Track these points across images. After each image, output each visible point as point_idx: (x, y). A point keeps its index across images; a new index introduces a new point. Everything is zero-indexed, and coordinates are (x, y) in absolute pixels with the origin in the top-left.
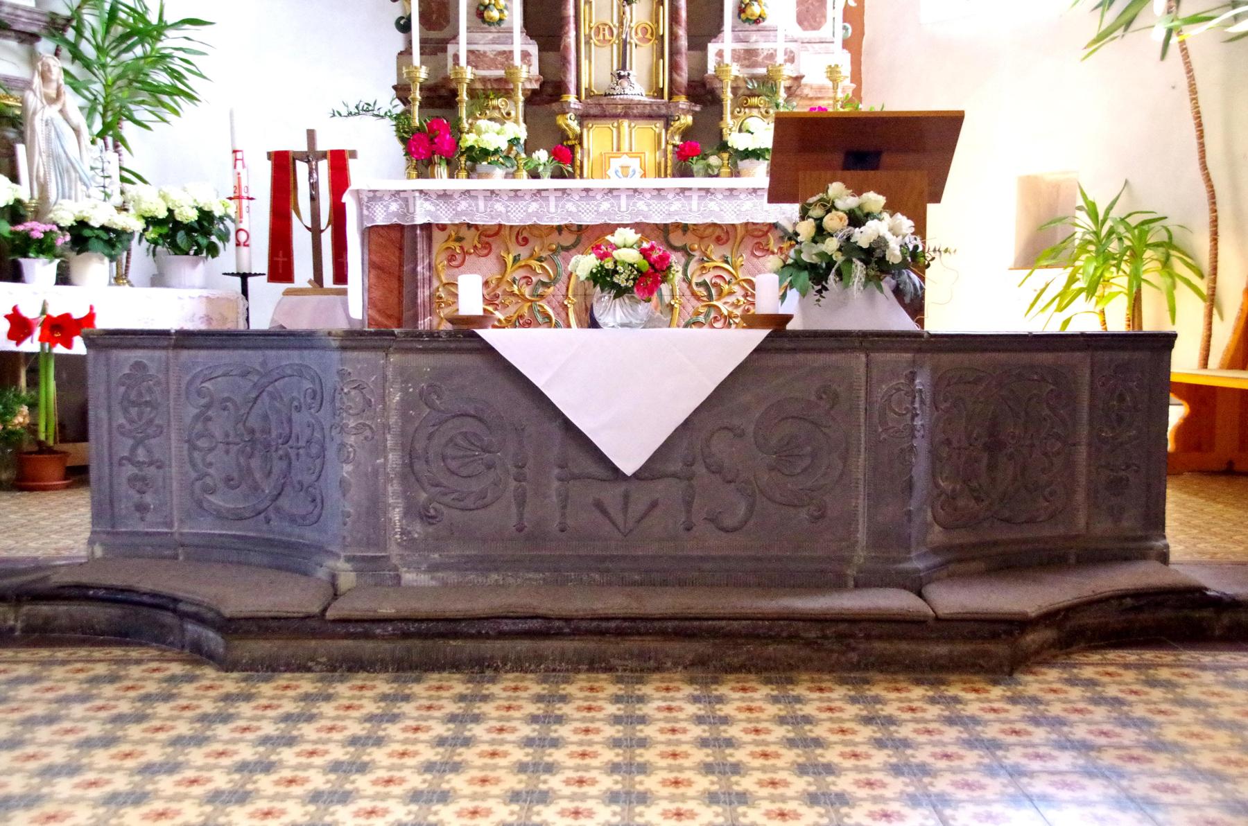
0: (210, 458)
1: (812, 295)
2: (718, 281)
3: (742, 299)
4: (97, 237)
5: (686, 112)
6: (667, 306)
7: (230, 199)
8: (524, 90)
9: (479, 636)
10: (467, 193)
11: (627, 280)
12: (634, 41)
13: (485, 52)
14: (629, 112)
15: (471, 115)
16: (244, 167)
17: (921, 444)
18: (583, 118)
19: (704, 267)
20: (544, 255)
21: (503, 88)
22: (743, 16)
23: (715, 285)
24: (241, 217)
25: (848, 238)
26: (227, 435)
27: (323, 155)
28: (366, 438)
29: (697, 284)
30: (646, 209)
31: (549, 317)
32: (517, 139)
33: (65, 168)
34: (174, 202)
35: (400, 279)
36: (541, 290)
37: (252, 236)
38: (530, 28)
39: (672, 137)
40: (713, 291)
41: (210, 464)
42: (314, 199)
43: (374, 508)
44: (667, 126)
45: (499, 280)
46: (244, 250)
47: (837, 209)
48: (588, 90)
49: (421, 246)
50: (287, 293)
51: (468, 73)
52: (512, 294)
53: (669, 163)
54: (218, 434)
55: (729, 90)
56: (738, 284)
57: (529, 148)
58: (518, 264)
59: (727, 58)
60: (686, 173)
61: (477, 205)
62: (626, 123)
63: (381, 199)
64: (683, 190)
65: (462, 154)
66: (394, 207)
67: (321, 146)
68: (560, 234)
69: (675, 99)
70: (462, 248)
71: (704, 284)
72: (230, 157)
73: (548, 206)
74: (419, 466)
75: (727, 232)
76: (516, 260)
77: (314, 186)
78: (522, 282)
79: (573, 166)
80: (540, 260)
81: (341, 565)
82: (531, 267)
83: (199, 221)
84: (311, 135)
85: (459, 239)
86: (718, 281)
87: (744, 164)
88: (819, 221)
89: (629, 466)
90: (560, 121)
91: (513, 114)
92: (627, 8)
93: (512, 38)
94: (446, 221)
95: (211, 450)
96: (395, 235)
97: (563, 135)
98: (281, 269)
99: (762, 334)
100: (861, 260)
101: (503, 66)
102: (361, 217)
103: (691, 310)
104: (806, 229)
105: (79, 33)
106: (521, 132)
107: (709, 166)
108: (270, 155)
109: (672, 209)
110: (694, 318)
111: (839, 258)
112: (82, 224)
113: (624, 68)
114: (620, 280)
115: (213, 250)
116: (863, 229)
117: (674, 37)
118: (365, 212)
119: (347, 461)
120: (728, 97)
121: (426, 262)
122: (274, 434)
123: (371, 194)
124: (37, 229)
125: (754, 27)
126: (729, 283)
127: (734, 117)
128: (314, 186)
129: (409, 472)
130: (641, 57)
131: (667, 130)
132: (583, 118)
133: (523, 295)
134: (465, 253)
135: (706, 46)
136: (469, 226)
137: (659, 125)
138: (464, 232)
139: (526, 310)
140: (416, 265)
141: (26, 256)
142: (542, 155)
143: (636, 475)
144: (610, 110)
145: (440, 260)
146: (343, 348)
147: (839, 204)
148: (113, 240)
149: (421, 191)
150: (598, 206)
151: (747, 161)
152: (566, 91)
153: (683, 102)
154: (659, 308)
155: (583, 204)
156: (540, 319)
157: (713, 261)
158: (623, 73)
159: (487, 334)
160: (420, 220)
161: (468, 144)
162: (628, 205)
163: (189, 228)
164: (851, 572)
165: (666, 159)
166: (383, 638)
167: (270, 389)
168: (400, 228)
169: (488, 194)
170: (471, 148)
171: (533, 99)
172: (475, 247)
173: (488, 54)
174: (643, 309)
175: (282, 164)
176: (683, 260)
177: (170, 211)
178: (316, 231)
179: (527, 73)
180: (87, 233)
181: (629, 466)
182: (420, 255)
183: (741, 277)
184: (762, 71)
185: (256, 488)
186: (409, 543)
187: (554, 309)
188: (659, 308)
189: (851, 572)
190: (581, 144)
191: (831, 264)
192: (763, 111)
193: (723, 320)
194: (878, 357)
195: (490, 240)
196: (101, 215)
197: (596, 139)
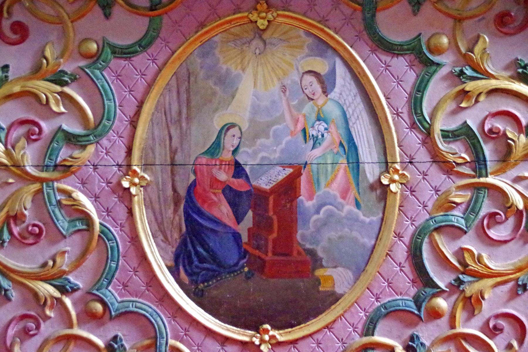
2: (499, 125)
6: (372, 188)
19: (464, 94)
29: (446, 135)
31: (87, 219)
40: (488, 150)
68: (107, 16)
78: (15, 134)
82: (36, 97)
86: (499, 125)
110: (439, 216)
133: (17, 166)
154: (353, 193)
156: (63, 224)
157: (490, 76)
176: (411, 77)
187: (95, 198)
188: (353, 193)
193: (511, 221)
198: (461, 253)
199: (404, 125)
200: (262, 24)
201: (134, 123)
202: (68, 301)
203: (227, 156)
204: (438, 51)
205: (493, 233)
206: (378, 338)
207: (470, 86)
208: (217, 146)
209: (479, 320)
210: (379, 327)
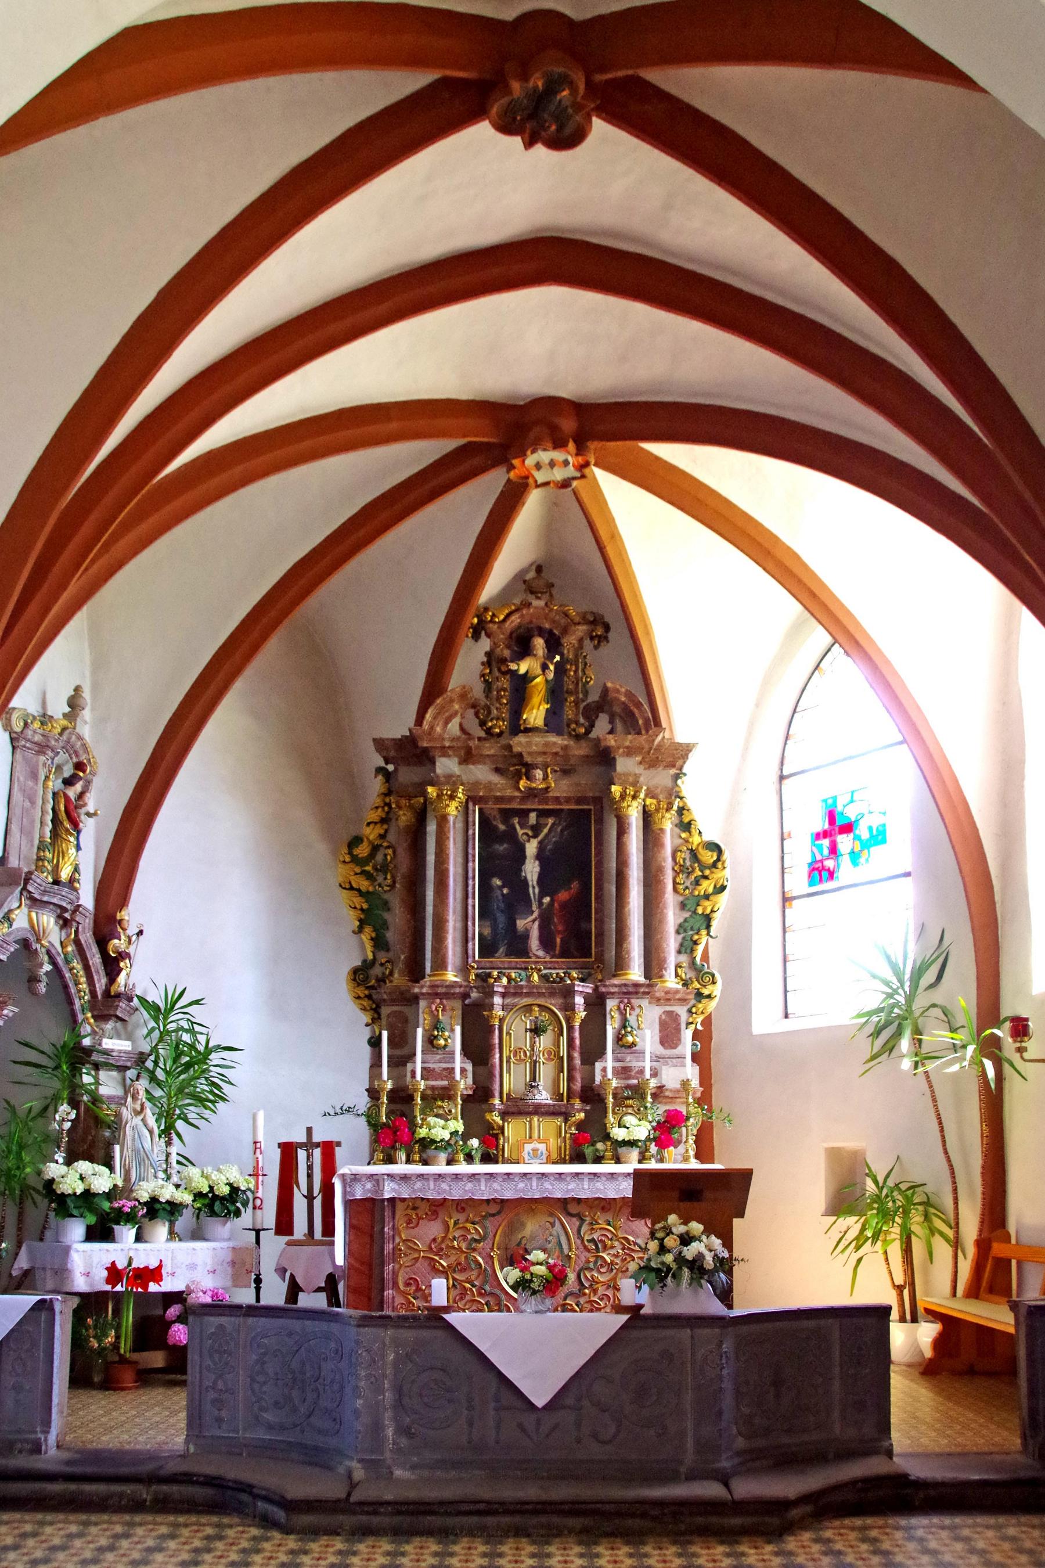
0: (264, 1389)
1: (658, 1287)
3: (621, 1251)
4: (164, 1209)
5: (579, 1111)
7: (250, 1175)
8: (462, 1095)
9: (447, 1514)
10: (421, 1176)
11: (539, 1286)
12: (542, 1060)
13: (434, 1069)
14: (539, 1110)
15: (423, 1112)
16: (261, 1153)
17: (727, 1385)
18: (504, 1115)
19: (593, 1229)
20: (477, 1220)
21: (446, 1094)
22: (620, 1043)
23: (601, 1241)
24: (258, 1188)
25: (680, 1253)
26: (277, 1374)
27: (318, 1145)
28: (372, 1383)
29: (588, 1241)
30: (550, 1187)
31: (480, 1264)
32: (457, 1132)
33: (142, 1157)
34: (213, 1181)
35: (372, 1236)
36: (474, 1245)
37: (264, 1202)
38: (467, 1051)
39: (570, 1128)
41: (265, 1392)
42: (310, 1176)
43: (377, 1427)
44: (566, 1121)
45: (444, 1238)
46: (258, 1212)
47: (673, 1234)
48: (508, 1095)
49: (387, 1213)
50: (289, 1244)
51: (422, 1085)
52: (453, 1247)
53: (568, 1147)
54: (270, 1371)
55: (611, 1096)
56: (618, 1240)
57: (466, 1136)
58: (457, 1226)
59: (610, 1075)
60: (578, 1158)
61: (428, 1185)
62: (536, 1119)
63: (359, 1180)
64: (577, 1174)
65: (416, 1142)
66: (369, 1186)
67: (316, 1138)
69: (572, 1102)
70: (417, 1215)
71: (593, 1241)
72: (252, 1146)
73: (479, 1185)
74: (406, 1401)
75: (609, 1203)
76: (456, 1223)
77: (310, 1168)
79: (497, 1150)
80: (473, 1223)
81: (354, 1464)
82: (466, 1228)
83: (230, 1194)
84: (309, 1130)
85: (415, 1208)
87: (622, 1150)
88: (662, 1240)
89: (540, 1402)
90: (488, 1117)
91: (453, 1111)
92: (537, 1039)
93: (454, 1058)
94: (406, 1196)
95: (265, 1383)
96: (368, 1205)
97: (490, 1126)
98: (284, 1225)
99: (624, 1318)
100: (688, 1268)
101: (447, 1078)
102: (345, 1193)
103: (583, 1259)
104: (653, 1246)
105: (156, 1063)
106: (459, 1126)
107: (597, 1150)
108: (280, 1145)
109: (569, 1187)
110: (586, 1265)
111: (674, 1266)
112: (154, 1199)
113: (533, 1079)
114: (535, 1286)
115: (238, 1213)
116: (689, 1247)
117: (570, 1058)
118: (348, 1189)
119: (359, 1397)
120: (610, 1100)
121: (391, 1225)
122: (308, 1375)
123: (353, 1177)
124: (127, 1205)
125: (628, 1051)
126: (611, 1240)
127: (614, 1113)
128: (310, 1168)
129: (399, 1405)
130: (546, 1072)
131: (566, 1123)
132: (504, 1115)
133: (460, 1248)
134: (420, 1218)
135: (594, 1065)
136: (423, 1199)
137: (559, 1121)
138: (418, 1203)
139: (463, 1260)
140: (383, 1228)
141: (118, 1224)
142: (475, 1143)
143: (545, 1407)
144: (523, 1109)
145: (401, 1224)
146: (359, 1326)
147: (674, 1230)
148: (173, 1208)
149: (388, 1175)
150: (516, 1186)
151: (624, 1148)
152: (493, 1096)
153: (577, 1104)
155: (505, 1184)
156: (473, 1266)
158: (533, 1084)
159: (451, 1318)
160: (387, 1196)
161: (422, 1136)
162: (537, 1186)
163: (222, 1199)
164: (683, 1469)
165: (565, 1146)
166: (385, 1514)
167: (306, 1345)
168: (371, 1200)
169: (437, 1177)
170: (424, 1139)
171: (466, 1099)
172: (426, 1214)
173: (436, 1070)
174: (549, 1302)
175: (288, 1151)
176: (578, 1223)
177: (211, 1188)
178: (310, 1198)
179: (464, 1084)
180: (157, 1206)
181: (540, 1402)
182: (387, 1220)
183: (620, 1236)
184: (635, 1082)
185: (295, 1410)
186: (398, 1450)
187: (483, 1259)
189: (683, 1469)
190: (503, 1133)
191: (669, 1269)
192: (636, 1109)
194: (699, 1331)
195: (438, 1209)
196: (167, 1193)
197: (513, 1130)
198: (592, 1276)
199: (576, 1237)
200: (534, 1207)
201: (495, 1236)
202: (474, 1289)
203: (523, 1246)
204: (586, 1216)
205: (602, 1270)
206: (568, 1302)
207: (594, 1227)
208: (520, 1243)
209: (597, 1296)
210: (569, 1298)
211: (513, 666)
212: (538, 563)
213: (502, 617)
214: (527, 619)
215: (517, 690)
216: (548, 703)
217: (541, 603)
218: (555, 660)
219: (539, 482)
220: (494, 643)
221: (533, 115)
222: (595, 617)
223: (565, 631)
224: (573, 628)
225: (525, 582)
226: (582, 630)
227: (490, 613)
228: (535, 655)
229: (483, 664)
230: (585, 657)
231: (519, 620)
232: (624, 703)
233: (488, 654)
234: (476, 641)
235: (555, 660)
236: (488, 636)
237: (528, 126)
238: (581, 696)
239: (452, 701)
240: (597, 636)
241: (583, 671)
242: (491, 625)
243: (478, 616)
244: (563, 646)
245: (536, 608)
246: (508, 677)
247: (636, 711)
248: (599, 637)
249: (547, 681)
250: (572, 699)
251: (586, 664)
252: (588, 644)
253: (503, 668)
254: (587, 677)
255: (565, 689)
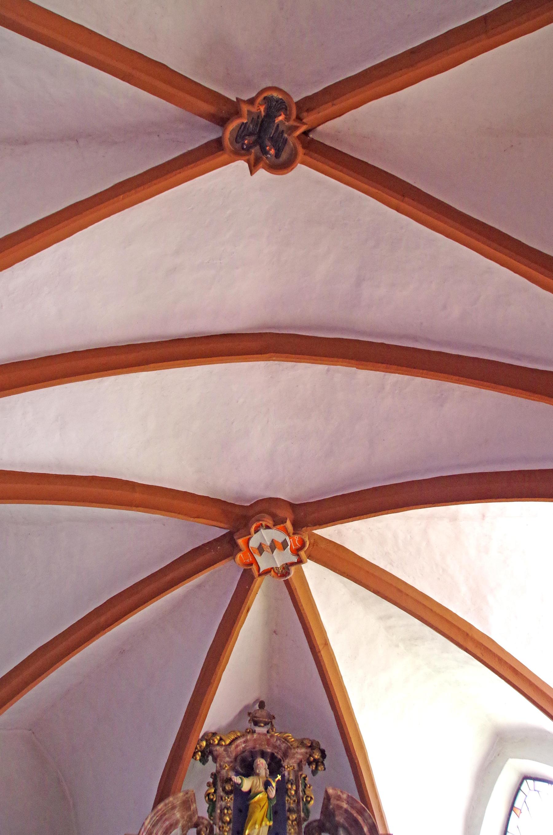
211: (237, 780)
212: (261, 700)
213: (228, 742)
214: (250, 745)
215: (240, 811)
216: (270, 820)
217: (264, 730)
218: (277, 779)
219: (263, 568)
220: (221, 766)
221: (259, 142)
222: (312, 743)
223: (286, 755)
224: (293, 751)
225: (249, 714)
226: (300, 752)
227: (218, 738)
228: (258, 775)
229: (209, 785)
230: (305, 778)
231: (243, 745)
232: (346, 811)
233: (214, 776)
234: (204, 764)
235: (277, 779)
236: (215, 760)
237: (253, 151)
238: (302, 815)
239: (173, 808)
240: (315, 760)
241: (304, 791)
242: (218, 748)
243: (207, 741)
244: (284, 768)
245: (259, 734)
246: (232, 796)
247: (360, 818)
248: (316, 761)
249: (269, 798)
250: (294, 816)
251: (305, 785)
252: (307, 770)
253: (228, 787)
254: (307, 796)
255: (287, 808)
